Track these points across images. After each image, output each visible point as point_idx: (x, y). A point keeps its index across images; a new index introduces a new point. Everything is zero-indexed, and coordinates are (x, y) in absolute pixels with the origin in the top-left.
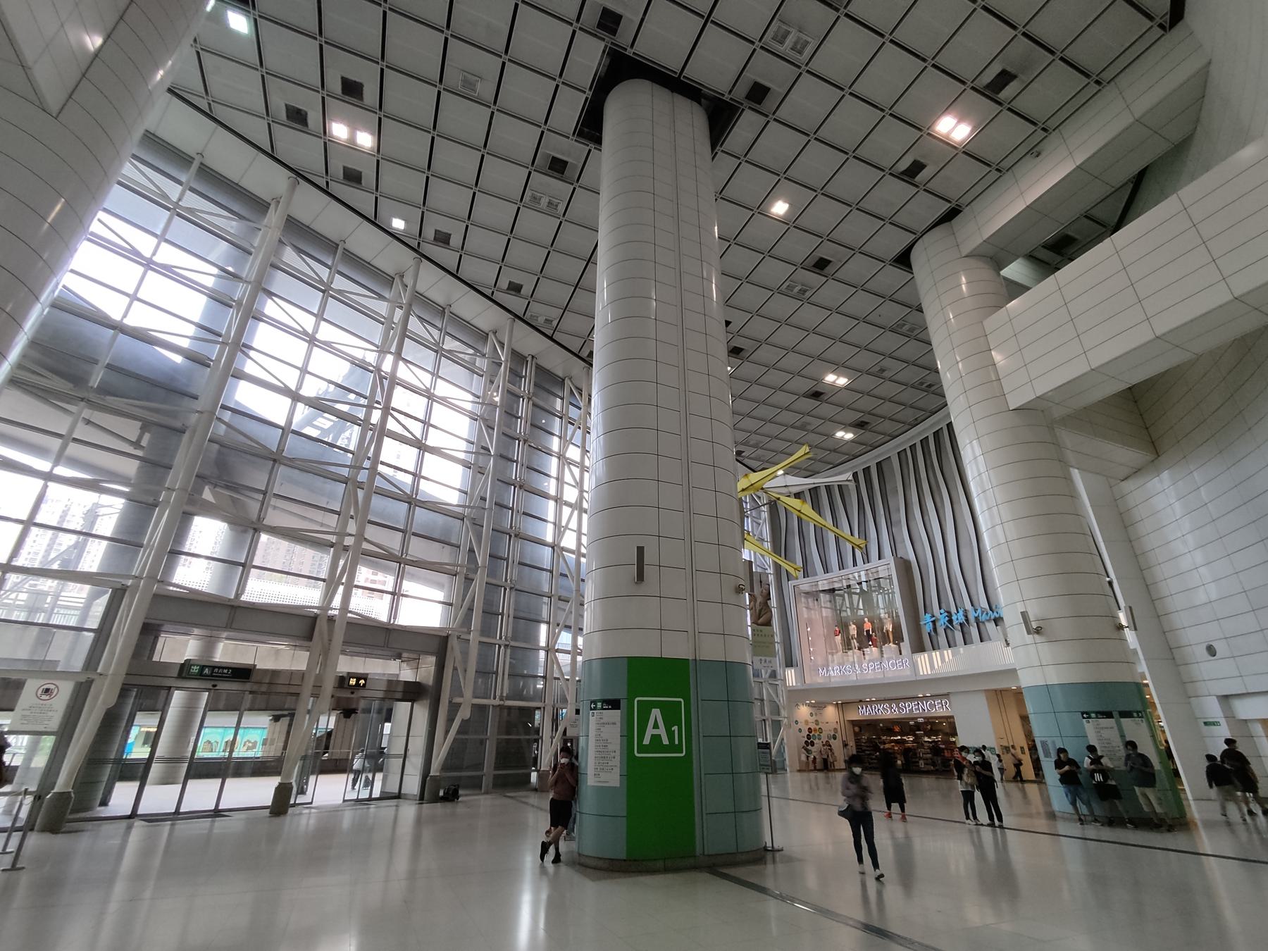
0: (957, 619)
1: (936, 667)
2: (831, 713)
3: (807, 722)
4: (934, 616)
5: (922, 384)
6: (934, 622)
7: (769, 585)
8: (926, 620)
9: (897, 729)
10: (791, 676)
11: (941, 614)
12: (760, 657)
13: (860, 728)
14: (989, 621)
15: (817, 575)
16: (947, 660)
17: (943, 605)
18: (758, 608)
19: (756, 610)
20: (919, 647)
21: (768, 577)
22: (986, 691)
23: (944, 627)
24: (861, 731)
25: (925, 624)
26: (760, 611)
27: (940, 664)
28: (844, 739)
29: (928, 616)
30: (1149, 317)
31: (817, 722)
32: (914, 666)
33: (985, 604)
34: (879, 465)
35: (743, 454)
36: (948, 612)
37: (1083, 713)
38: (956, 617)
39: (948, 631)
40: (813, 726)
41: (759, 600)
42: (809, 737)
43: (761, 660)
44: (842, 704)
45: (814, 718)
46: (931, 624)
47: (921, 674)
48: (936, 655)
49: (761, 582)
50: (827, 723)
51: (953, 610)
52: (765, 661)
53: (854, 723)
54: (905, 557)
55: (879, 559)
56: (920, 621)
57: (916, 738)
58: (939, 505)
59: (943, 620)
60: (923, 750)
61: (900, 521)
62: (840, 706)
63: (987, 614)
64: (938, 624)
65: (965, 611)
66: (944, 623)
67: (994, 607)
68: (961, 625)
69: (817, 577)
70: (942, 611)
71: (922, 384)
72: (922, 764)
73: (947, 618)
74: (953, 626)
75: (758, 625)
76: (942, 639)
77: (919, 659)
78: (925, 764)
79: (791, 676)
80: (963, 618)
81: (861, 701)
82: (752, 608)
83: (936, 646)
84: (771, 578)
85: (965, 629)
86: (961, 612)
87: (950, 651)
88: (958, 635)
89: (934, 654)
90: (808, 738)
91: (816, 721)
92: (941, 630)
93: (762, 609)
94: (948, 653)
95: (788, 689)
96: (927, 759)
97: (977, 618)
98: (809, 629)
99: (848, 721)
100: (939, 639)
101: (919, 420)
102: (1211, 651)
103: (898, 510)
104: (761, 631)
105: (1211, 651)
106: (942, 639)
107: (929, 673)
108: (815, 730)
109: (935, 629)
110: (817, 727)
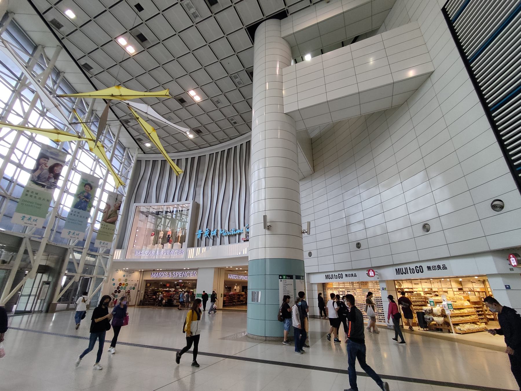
0: (213, 234)
1: (197, 255)
2: (136, 276)
3: (120, 280)
4: (203, 231)
5: (232, 120)
6: (202, 234)
7: (121, 202)
8: (199, 232)
9: (168, 285)
10: (118, 255)
11: (206, 230)
12: (101, 241)
13: (150, 284)
14: (226, 236)
17: (208, 227)
18: (109, 212)
19: (107, 213)
20: (191, 245)
21: (122, 197)
22: (215, 268)
23: (206, 237)
24: (150, 286)
25: (198, 234)
26: (110, 215)
27: (199, 254)
28: (139, 289)
29: (200, 231)
30: (357, 84)
31: (126, 280)
33: (226, 228)
34: (199, 157)
35: (129, 124)
36: (209, 230)
37: (280, 276)
39: (207, 239)
40: (122, 282)
41: (112, 208)
42: (118, 288)
43: (101, 242)
44: (144, 271)
45: (125, 278)
46: (200, 234)
48: (198, 249)
49: (117, 199)
50: (132, 281)
51: (212, 230)
52: (104, 243)
53: (147, 282)
54: (198, 202)
56: (195, 233)
58: (220, 181)
59: (206, 233)
60: (177, 295)
61: (201, 185)
62: (142, 272)
63: (226, 233)
64: (203, 235)
65: (217, 230)
66: (207, 235)
67: (230, 230)
68: (214, 237)
70: (207, 229)
71: (232, 120)
73: (208, 233)
74: (210, 237)
75: (106, 222)
76: (203, 242)
77: (190, 251)
78: (176, 302)
79: (118, 255)
80: (216, 233)
81: (154, 270)
82: (105, 212)
83: (199, 245)
84: (124, 198)
85: (214, 239)
86: (215, 231)
87: (205, 248)
88: (211, 241)
89: (197, 249)
90: (118, 289)
91: (126, 279)
92: (204, 238)
93: (112, 214)
94: (204, 249)
97: (221, 234)
98: (138, 230)
100: (202, 242)
101: (225, 140)
102: (310, 254)
103: (202, 180)
104: (107, 226)
105: (310, 254)
106: (203, 242)
107: (193, 257)
108: (124, 284)
109: (201, 237)
110: (125, 283)
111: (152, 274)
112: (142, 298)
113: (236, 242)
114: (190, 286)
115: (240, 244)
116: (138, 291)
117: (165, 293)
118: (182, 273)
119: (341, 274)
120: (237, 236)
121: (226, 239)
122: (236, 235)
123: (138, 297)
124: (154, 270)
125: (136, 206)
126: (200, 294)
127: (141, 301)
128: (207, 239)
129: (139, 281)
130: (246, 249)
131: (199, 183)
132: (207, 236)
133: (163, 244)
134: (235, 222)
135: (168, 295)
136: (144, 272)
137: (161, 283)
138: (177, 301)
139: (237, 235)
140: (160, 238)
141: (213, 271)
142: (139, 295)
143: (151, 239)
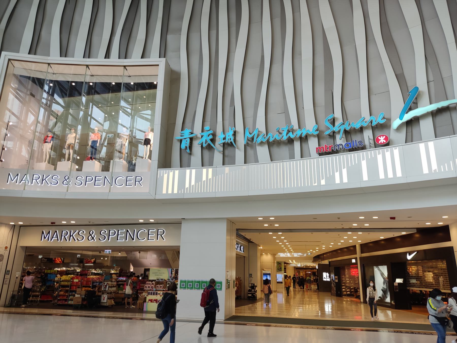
1: (187, 185)
6: (191, 139)
14: (262, 143)
15: (49, 56)
16: (204, 178)
27: (193, 183)
28: (9, 268)
32: (157, 183)
46: (189, 140)
47: (164, 192)
54: (174, 67)
55: (142, 58)
57: (83, 270)
60: (110, 283)
61: (180, 30)
62: (17, 229)
66: (206, 141)
68: (225, 145)
69: (49, 58)
72: (105, 299)
73: (211, 137)
77: (166, 176)
78: (108, 298)
88: (218, 157)
92: (197, 149)
96: (111, 293)
99: (22, 247)
103: (182, 18)
107: (176, 191)
111: (43, 233)
112: (17, 289)
114: (109, 264)
115: (306, 162)
116: (7, 272)
117: (77, 278)
118: (128, 231)
120: (297, 145)
121: (263, 151)
122: (290, 141)
123: (5, 287)
125: (9, 60)
126: (189, 282)
127: (13, 297)
128: (206, 153)
129: (8, 249)
130: (345, 171)
131: (173, 24)
132: (209, 144)
133: (80, 163)
134: (286, 112)
135: (85, 283)
136: (21, 227)
137: (40, 257)
138: (109, 295)
139: (295, 142)
140: (69, 148)
141: (223, 227)
142: (8, 282)
143: (44, 150)
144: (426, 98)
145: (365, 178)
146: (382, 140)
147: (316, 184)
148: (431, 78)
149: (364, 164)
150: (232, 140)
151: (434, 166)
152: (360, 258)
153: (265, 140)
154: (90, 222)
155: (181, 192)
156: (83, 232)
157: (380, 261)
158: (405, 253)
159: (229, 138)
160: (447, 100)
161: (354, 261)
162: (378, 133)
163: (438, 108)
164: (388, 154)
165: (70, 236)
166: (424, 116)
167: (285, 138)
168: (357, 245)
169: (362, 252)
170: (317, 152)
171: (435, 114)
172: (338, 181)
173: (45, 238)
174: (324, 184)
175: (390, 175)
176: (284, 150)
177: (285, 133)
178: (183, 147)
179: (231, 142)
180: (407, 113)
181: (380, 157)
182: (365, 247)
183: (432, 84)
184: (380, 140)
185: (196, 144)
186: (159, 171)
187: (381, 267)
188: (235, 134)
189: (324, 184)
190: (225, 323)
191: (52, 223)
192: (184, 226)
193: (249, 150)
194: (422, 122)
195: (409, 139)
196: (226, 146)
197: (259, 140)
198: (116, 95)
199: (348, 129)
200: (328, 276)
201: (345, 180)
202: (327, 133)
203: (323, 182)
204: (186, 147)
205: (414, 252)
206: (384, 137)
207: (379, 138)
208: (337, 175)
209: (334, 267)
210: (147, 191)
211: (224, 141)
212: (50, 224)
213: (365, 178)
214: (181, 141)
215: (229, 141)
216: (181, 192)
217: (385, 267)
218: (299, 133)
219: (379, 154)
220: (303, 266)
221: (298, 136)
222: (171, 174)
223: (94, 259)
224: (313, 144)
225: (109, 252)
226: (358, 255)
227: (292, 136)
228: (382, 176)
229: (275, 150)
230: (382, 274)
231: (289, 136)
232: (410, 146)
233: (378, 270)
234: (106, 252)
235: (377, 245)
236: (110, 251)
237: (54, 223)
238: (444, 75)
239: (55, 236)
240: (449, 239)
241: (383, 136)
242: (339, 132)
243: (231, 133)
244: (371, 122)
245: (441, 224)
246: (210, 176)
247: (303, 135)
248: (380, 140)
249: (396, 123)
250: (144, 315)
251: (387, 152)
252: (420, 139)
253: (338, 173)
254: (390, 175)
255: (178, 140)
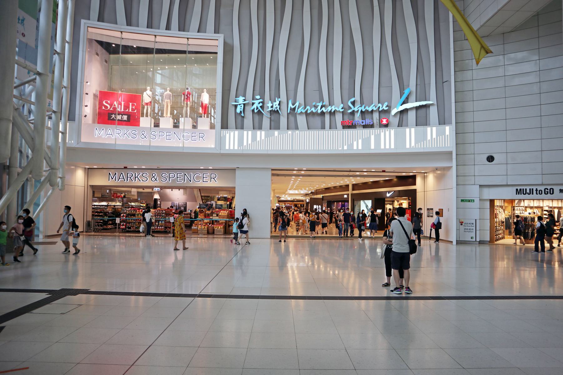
0: (272, 107)
1: (245, 144)
6: (244, 104)
16: (258, 139)
27: (250, 142)
29: (241, 99)
32: (220, 141)
38: (271, 105)
44: (88, 168)
46: (242, 105)
47: (227, 147)
53: (94, 188)
62: (87, 170)
66: (257, 108)
73: (261, 104)
77: (227, 135)
81: (125, 168)
88: (266, 122)
95: (68, 146)
107: (236, 148)
113: (323, 127)
119: (550, 189)
120: (327, 117)
121: (302, 120)
124: (125, 168)
128: (257, 117)
130: (360, 141)
132: (259, 110)
144: (413, 97)
145: (373, 147)
146: (384, 121)
147: (341, 149)
148: (419, 83)
149: (373, 137)
150: (278, 109)
151: (413, 144)
152: (351, 194)
153: (304, 111)
154: (158, 167)
155: (240, 148)
156: (147, 174)
157: (365, 197)
158: (386, 192)
159: (276, 106)
160: (426, 101)
161: (346, 196)
162: (383, 116)
163: (420, 105)
164: (387, 133)
165: (136, 178)
166: (411, 109)
167: (319, 111)
168: (350, 185)
169: (353, 190)
170: (342, 125)
171: (417, 108)
172: (355, 148)
173: (112, 179)
174: (346, 149)
175: (387, 147)
176: (318, 120)
177: (319, 107)
178: (238, 111)
179: (277, 110)
180: (401, 105)
181: (382, 134)
182: (355, 187)
183: (418, 86)
184: (383, 121)
185: (249, 109)
186: (222, 131)
187: (366, 201)
188: (279, 104)
189: (346, 149)
190: (270, 239)
191: (125, 167)
192: (237, 172)
193: (292, 118)
194: (409, 112)
195: (400, 125)
196: (272, 112)
197: (299, 111)
198: (168, 56)
199: (364, 110)
200: (320, 208)
201: (360, 147)
202: (350, 111)
203: (345, 148)
204: (241, 112)
205: (392, 191)
206: (386, 119)
207: (383, 120)
208: (355, 143)
209: (327, 201)
210: (213, 146)
211: (272, 109)
212: (123, 168)
213: (373, 147)
214: (236, 106)
215: (276, 110)
216: (240, 148)
217: (370, 201)
218: (329, 109)
219: (382, 132)
220: (293, 199)
221: (329, 111)
222: (232, 134)
223: (124, 194)
224: (339, 118)
225: (158, 189)
226: (350, 192)
227: (325, 111)
228: (382, 147)
229: (311, 119)
230: (367, 206)
231: (323, 110)
232: (400, 129)
233: (364, 204)
234: (155, 189)
235: (365, 185)
236: (159, 189)
237: (126, 167)
238: (426, 83)
239: (122, 177)
240: (415, 184)
241: (385, 119)
242: (358, 111)
243: (277, 102)
244: (379, 108)
245: (411, 174)
246: (263, 137)
247: (333, 111)
248: (383, 121)
249: (394, 112)
250: (215, 236)
251: (387, 131)
252: (407, 126)
253: (356, 142)
254: (387, 147)
255: (233, 105)
